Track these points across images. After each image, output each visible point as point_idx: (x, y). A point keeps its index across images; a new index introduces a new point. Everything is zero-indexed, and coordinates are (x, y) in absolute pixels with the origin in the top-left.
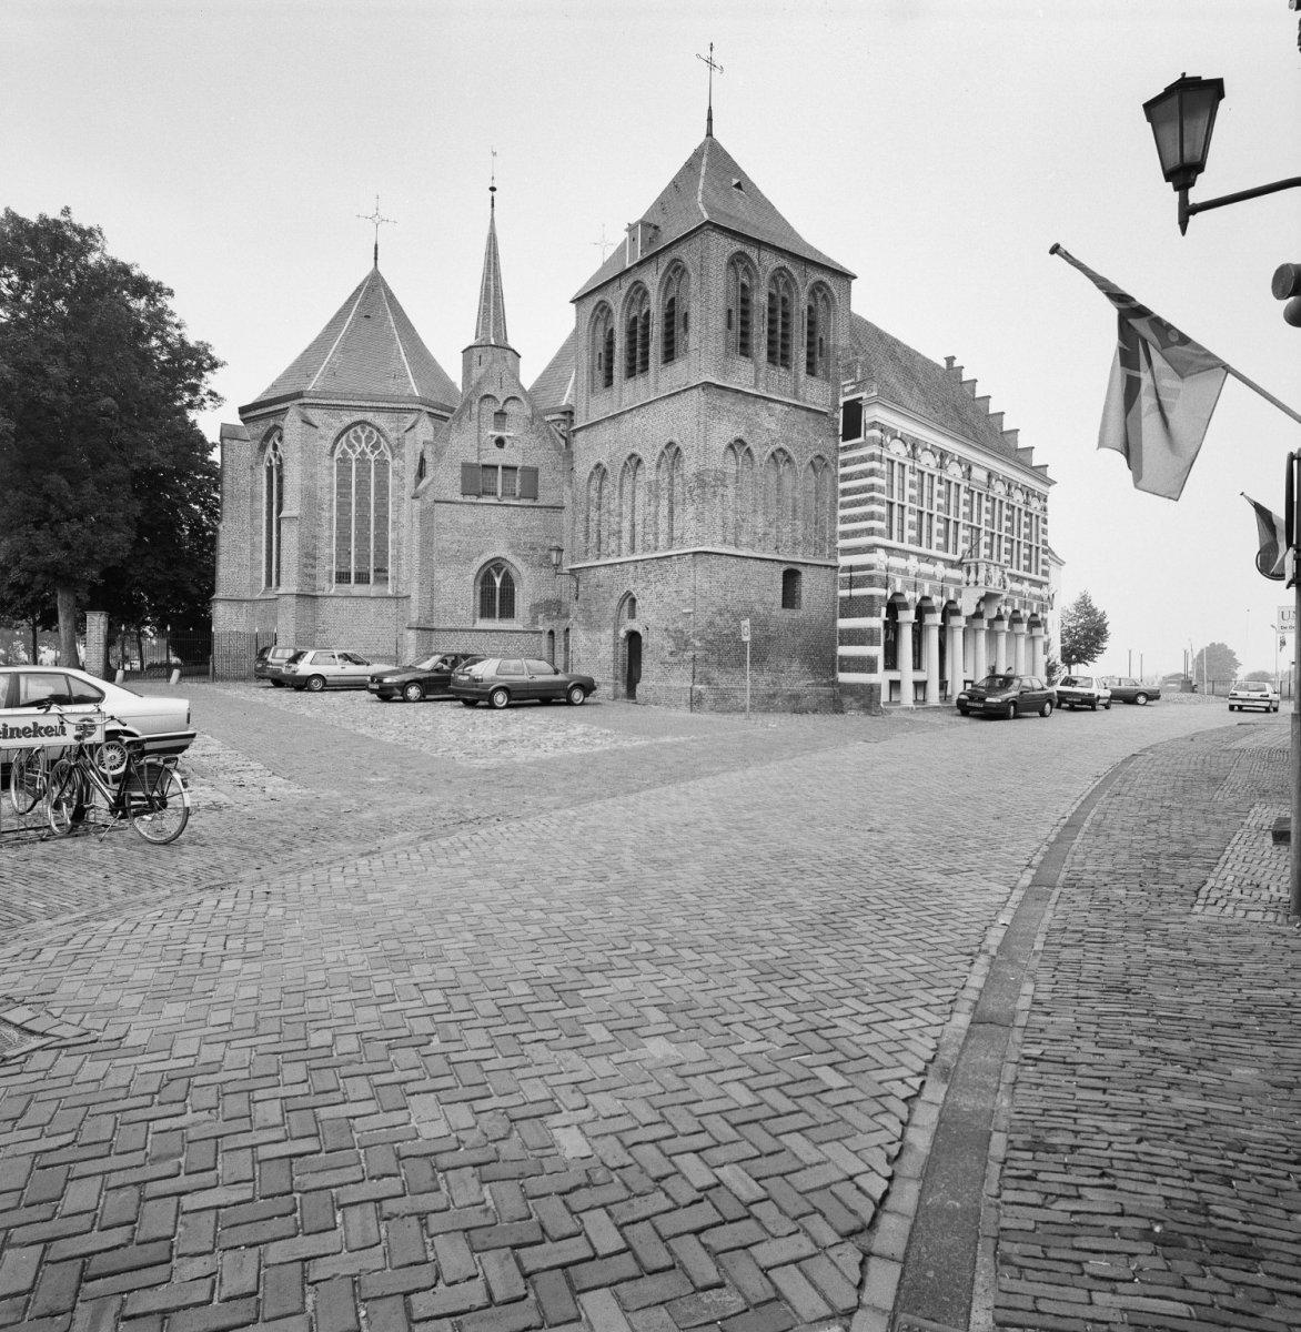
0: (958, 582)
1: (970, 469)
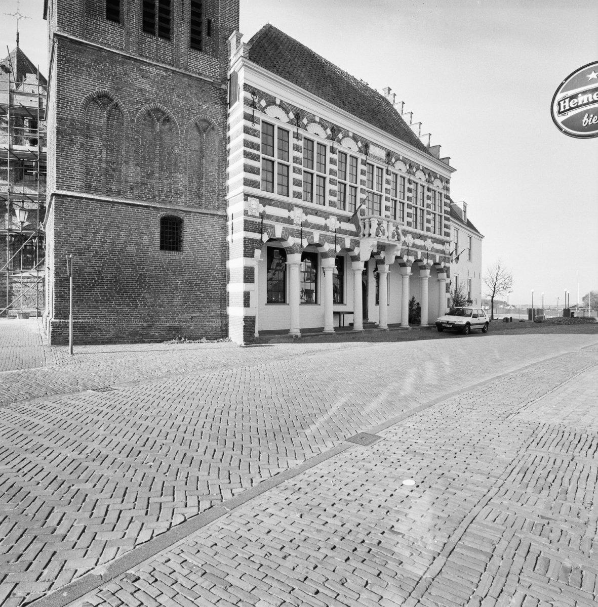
0: (351, 233)
1: (366, 146)
